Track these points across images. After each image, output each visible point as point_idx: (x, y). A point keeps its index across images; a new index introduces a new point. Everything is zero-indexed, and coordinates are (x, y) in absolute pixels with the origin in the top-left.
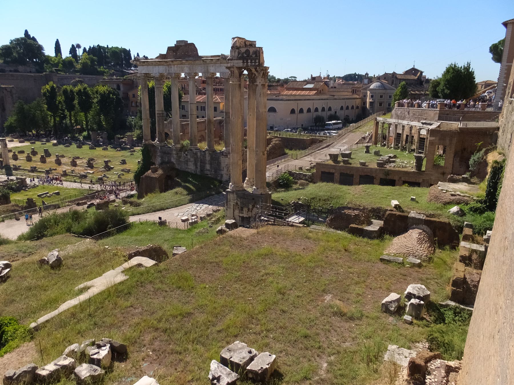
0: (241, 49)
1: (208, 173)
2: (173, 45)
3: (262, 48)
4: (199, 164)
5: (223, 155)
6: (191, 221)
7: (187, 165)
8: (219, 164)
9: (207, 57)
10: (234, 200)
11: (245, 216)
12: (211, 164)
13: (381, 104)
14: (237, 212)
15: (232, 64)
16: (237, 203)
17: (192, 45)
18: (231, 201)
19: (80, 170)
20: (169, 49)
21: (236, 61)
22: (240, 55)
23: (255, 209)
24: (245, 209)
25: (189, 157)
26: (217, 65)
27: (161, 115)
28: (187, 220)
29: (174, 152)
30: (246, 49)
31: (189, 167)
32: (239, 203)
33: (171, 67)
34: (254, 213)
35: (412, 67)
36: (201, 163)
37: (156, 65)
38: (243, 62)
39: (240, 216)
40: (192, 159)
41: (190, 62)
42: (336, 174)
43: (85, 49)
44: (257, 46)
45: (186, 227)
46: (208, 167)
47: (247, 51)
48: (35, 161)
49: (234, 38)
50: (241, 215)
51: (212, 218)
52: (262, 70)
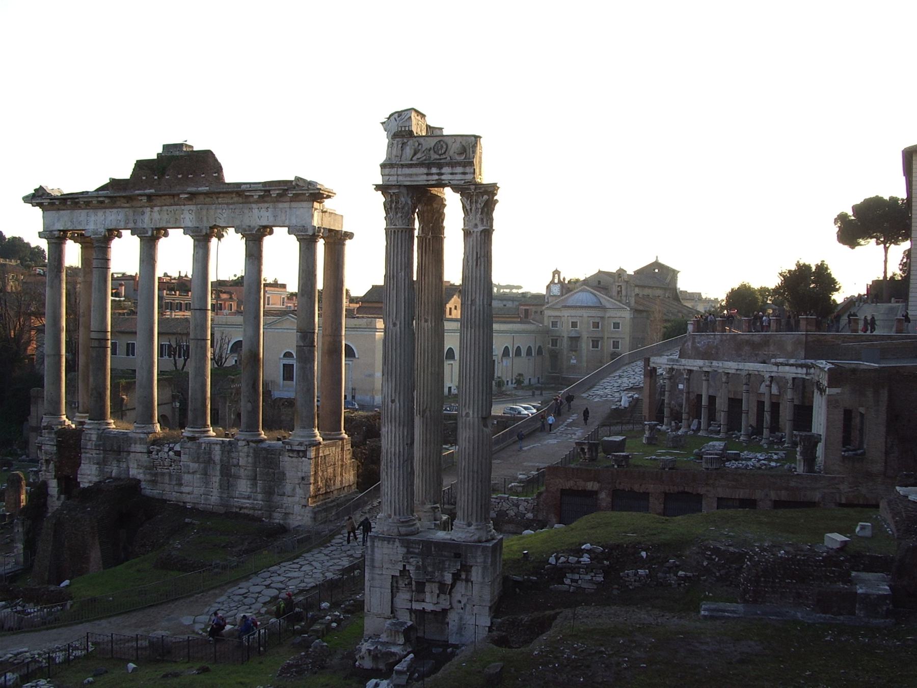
0: (422, 140)
1: (247, 503)
2: (151, 153)
3: (480, 137)
4: (216, 480)
5: (292, 451)
7: (181, 485)
11: (429, 607)
12: (254, 479)
13: (595, 344)
14: (403, 597)
16: (404, 572)
17: (207, 156)
20: (141, 166)
21: (407, 171)
22: (418, 156)
23: (460, 587)
24: (431, 589)
26: (280, 205)
31: (185, 489)
33: (143, 213)
34: (457, 596)
35: (654, 260)
36: (222, 474)
37: (95, 208)
39: (411, 610)
40: (194, 466)
41: (201, 198)
42: (603, 495)
46: (243, 486)
50: (417, 606)
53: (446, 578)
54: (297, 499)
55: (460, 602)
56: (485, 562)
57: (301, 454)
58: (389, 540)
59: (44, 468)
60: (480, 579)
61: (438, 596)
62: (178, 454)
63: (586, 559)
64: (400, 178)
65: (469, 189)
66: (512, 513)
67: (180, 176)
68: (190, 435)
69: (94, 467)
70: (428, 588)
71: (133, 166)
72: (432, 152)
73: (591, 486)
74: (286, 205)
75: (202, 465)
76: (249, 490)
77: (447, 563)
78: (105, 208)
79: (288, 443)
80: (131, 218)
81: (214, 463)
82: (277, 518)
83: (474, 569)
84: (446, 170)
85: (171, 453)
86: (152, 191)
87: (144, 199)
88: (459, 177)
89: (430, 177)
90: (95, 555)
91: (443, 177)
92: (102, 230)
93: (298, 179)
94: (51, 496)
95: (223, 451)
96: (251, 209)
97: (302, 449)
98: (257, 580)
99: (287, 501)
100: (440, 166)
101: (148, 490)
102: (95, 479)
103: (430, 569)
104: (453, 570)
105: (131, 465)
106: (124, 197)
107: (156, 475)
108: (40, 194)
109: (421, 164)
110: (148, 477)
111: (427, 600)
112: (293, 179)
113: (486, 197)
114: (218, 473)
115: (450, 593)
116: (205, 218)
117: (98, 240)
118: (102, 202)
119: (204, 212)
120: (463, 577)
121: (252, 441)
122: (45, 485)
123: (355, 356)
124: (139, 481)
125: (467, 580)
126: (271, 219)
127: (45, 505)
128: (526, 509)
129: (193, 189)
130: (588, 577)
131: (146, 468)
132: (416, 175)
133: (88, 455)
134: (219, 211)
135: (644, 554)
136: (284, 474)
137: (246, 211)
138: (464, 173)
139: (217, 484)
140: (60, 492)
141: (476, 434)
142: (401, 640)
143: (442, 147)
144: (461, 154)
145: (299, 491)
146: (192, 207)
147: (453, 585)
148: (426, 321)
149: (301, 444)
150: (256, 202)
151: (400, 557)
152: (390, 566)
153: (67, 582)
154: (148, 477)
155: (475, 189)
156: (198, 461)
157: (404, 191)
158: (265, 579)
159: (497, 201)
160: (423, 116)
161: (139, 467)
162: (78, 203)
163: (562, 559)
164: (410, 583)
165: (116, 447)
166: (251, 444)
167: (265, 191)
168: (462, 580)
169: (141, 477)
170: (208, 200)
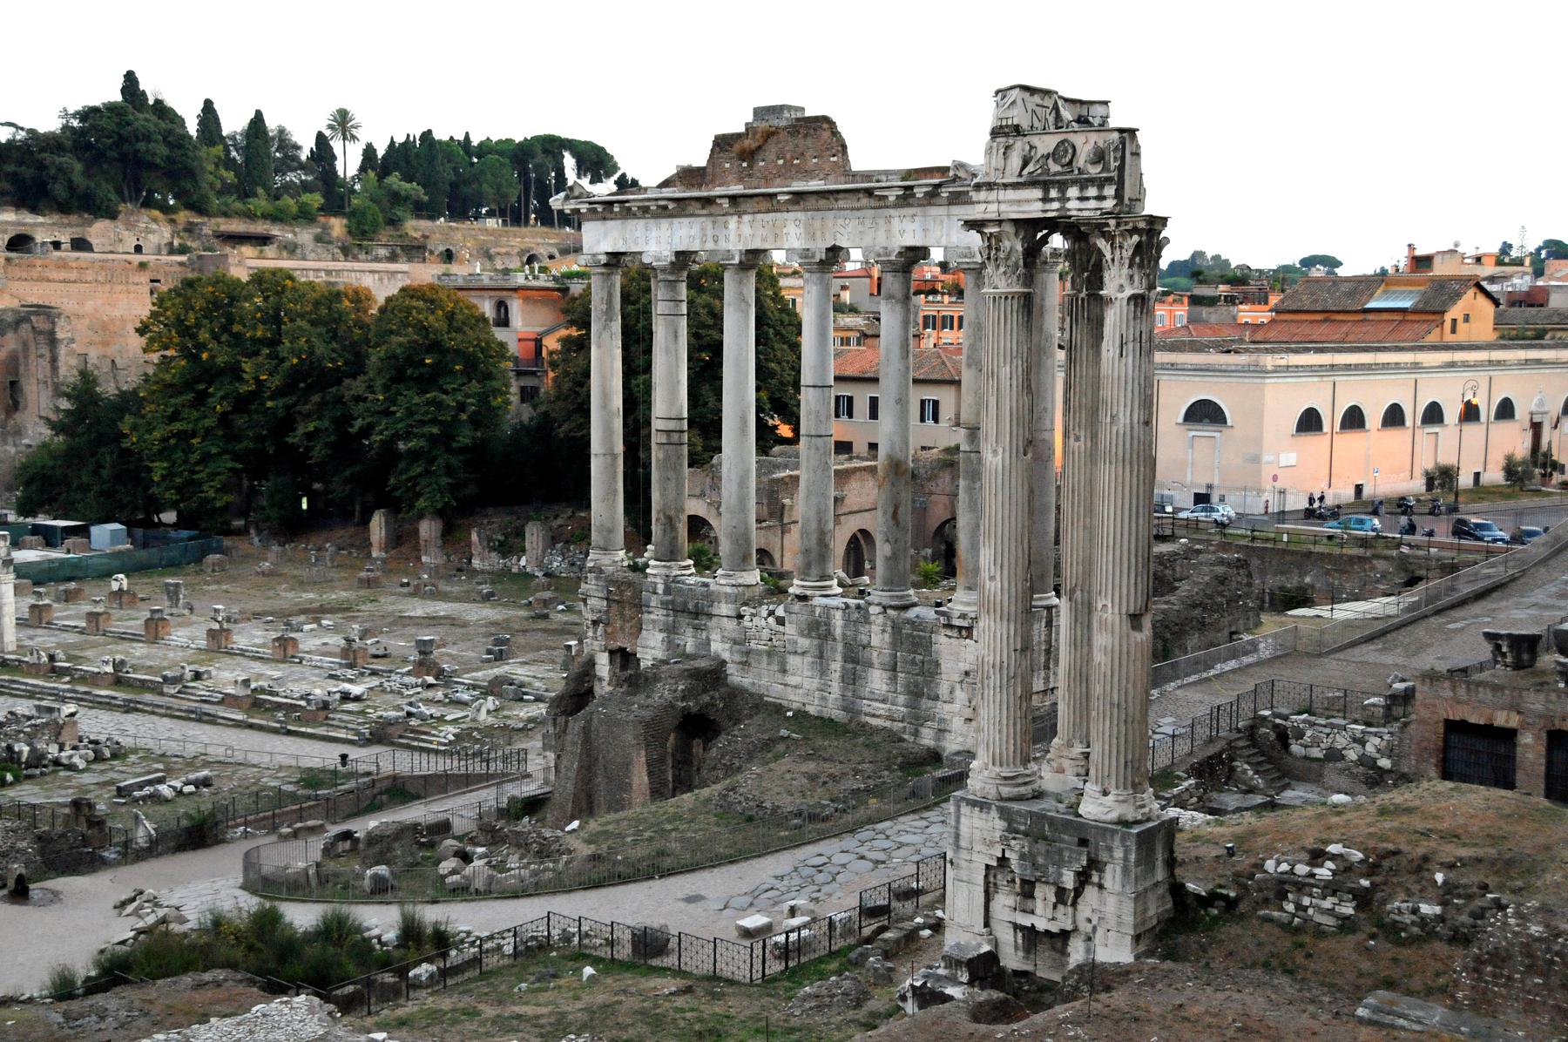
1: (881, 708)
4: (836, 666)
5: (949, 626)
6: (781, 939)
7: (784, 671)
8: (930, 670)
9: (887, 173)
10: (991, 844)
11: (1041, 925)
12: (893, 669)
14: (1004, 902)
15: (993, 207)
16: (1003, 861)
18: (977, 847)
19: (305, 683)
20: (722, 143)
21: (1011, 194)
22: (1030, 168)
23: (1090, 892)
24: (1045, 894)
25: (790, 629)
26: (934, 211)
27: (675, 437)
28: (767, 929)
29: (725, 609)
30: (1060, 138)
32: (1012, 856)
34: (1084, 910)
37: (656, 216)
38: (1046, 199)
39: (1016, 927)
40: (804, 643)
41: (812, 202)
42: (1526, 739)
43: (369, 151)
44: (1114, 122)
45: (758, 966)
46: (877, 680)
47: (1064, 152)
48: (122, 638)
49: (1001, 93)
50: (1026, 921)
51: (883, 929)
52: (1135, 230)
53: (1064, 878)
54: (956, 707)
55: (1090, 921)
56: (1126, 859)
57: (964, 633)
58: (982, 805)
59: (590, 634)
60: (1118, 887)
61: (1055, 907)
62: (781, 621)
63: (1325, 872)
64: (1003, 207)
65: (1107, 225)
66: (1352, 755)
67: (781, 162)
68: (798, 591)
69: (660, 636)
70: (1039, 891)
71: (710, 146)
72: (1050, 161)
73: (1501, 719)
74: (942, 210)
75: (816, 642)
76: (885, 687)
77: (1067, 854)
78: (672, 216)
79: (943, 614)
80: (710, 232)
81: (834, 640)
82: (927, 739)
83: (1109, 868)
84: (1073, 192)
85: (771, 619)
86: (737, 189)
87: (725, 203)
88: (1092, 204)
89: (1048, 206)
90: (640, 778)
91: (1070, 205)
92: (667, 256)
93: (960, 166)
94: (600, 679)
95: (847, 620)
96: (889, 219)
97: (965, 624)
98: (849, 842)
99: (943, 709)
100: (1062, 186)
101: (735, 676)
102: (660, 655)
103: (1040, 860)
104: (1077, 867)
105: (713, 637)
106: (697, 199)
107: (748, 653)
108: (576, 193)
109: (1032, 183)
110: (737, 658)
111: (1039, 911)
112: (948, 163)
113: (1136, 238)
114: (839, 657)
115: (1074, 904)
116: (818, 234)
117: (663, 270)
118: (665, 208)
119: (817, 224)
120: (1095, 879)
121: (892, 607)
122: (591, 663)
123: (1224, 421)
124: (724, 663)
125: (1101, 887)
126: (919, 234)
127: (590, 692)
128: (1379, 751)
129: (798, 186)
130: (1327, 903)
131: (735, 642)
132: (1028, 201)
133: (652, 617)
134: (840, 221)
135: (1439, 877)
136: (938, 664)
137: (881, 222)
138: (1100, 198)
139: (837, 675)
140: (613, 674)
141: (1117, 643)
142: (965, 978)
143: (1066, 151)
144: (1094, 163)
145: (961, 696)
146: (801, 215)
147: (1078, 892)
148: (1077, 439)
149: (963, 616)
150: (895, 206)
151: (998, 834)
152: (984, 849)
153: (575, 824)
154: (737, 658)
155: (1118, 225)
156: (809, 636)
157: (1009, 228)
158: (863, 843)
159: (1167, 240)
160: (1047, 93)
161: (724, 639)
162: (629, 209)
163: (1284, 867)
164: (1013, 881)
165: (691, 610)
166: (890, 612)
167: (906, 188)
168: (1093, 884)
169: (726, 656)
170: (822, 203)
